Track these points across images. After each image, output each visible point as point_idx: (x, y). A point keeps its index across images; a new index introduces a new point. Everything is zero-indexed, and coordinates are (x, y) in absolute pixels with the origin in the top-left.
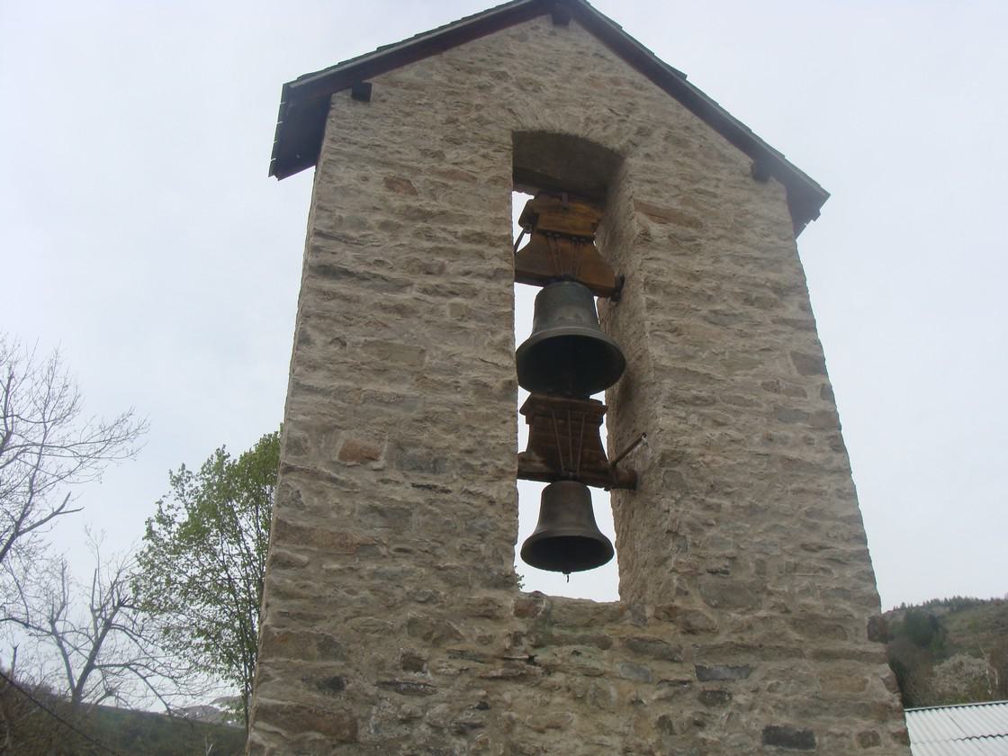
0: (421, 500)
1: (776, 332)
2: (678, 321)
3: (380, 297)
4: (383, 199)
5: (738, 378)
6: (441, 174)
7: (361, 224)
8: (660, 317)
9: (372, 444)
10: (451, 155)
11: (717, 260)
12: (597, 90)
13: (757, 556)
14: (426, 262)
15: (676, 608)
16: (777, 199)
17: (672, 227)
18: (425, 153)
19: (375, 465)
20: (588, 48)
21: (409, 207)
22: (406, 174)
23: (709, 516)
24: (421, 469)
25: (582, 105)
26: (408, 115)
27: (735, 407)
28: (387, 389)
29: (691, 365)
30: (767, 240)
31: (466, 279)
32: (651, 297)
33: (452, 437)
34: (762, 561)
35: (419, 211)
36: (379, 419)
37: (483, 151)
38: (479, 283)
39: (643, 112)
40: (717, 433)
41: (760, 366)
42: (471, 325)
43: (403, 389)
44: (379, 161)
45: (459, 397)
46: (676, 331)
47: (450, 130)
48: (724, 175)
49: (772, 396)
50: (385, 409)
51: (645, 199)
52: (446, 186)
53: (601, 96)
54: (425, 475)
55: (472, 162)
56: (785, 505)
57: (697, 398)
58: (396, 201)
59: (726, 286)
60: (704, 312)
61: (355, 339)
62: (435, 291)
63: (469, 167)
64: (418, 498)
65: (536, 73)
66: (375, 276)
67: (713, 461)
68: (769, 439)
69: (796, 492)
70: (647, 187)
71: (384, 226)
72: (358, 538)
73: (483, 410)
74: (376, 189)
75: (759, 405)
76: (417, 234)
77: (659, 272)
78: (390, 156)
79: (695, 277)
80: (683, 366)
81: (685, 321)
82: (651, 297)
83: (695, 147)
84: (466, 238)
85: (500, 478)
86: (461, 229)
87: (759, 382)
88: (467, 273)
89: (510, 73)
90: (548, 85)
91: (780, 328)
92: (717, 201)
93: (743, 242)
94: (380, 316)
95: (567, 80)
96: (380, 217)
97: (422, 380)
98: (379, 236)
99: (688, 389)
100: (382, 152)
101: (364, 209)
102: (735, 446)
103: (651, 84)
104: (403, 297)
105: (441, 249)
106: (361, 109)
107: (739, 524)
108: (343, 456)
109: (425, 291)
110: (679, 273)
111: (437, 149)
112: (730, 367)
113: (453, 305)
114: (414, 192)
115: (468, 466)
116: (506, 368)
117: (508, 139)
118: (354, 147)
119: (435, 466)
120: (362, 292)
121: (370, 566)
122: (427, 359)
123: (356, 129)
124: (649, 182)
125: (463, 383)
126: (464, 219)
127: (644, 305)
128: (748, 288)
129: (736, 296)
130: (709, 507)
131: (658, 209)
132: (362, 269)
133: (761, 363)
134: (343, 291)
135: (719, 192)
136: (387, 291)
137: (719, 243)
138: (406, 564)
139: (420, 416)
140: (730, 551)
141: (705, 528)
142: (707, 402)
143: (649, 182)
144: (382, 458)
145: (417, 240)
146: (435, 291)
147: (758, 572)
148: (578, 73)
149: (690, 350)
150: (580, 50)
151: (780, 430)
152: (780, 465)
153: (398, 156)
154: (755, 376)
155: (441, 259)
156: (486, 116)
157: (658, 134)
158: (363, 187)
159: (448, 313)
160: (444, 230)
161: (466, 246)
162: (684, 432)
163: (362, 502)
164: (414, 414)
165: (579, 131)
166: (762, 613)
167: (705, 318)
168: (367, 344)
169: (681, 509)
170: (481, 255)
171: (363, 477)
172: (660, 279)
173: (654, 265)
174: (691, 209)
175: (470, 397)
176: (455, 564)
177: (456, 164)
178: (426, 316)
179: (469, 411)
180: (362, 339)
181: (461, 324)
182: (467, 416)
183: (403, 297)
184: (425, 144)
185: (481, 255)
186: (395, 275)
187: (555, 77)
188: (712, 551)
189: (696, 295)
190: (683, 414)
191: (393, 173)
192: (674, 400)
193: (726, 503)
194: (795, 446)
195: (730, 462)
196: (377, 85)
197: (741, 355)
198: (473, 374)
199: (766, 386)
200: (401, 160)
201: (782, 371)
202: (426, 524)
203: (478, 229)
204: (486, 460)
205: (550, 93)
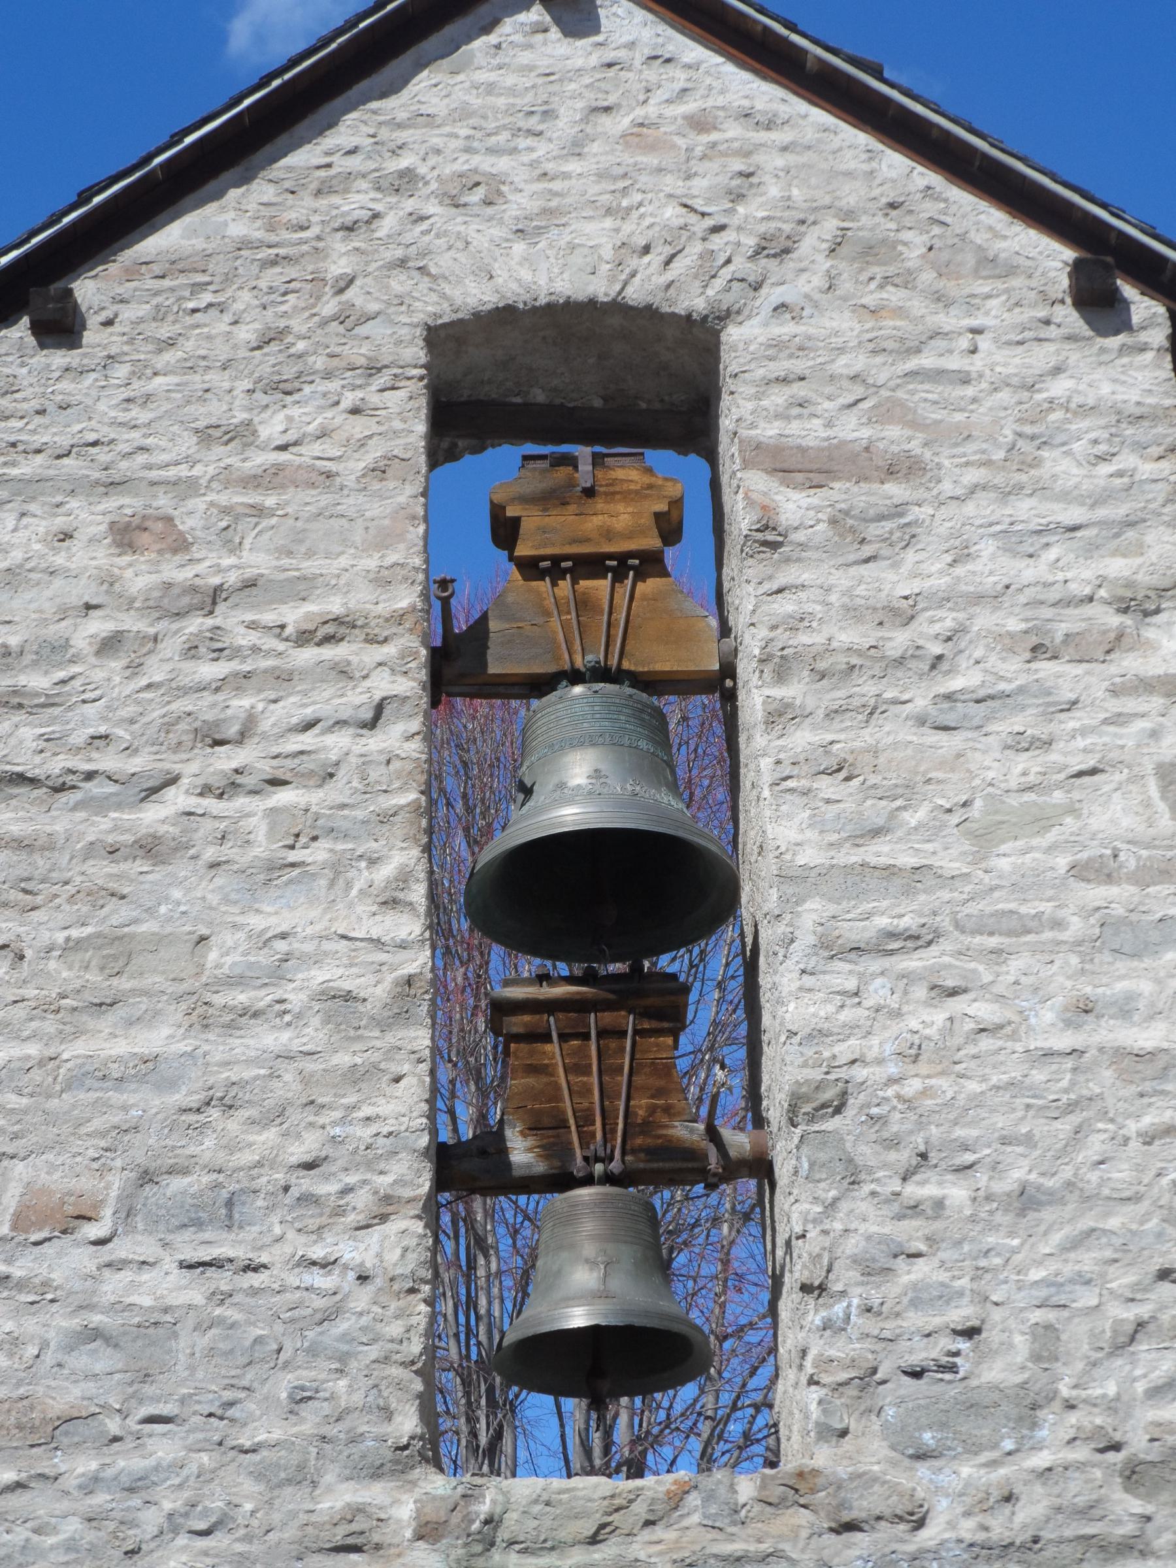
0: (196, 1297)
1: (1118, 720)
2: (849, 738)
3: (101, 827)
4: (109, 581)
5: (1004, 864)
6: (254, 481)
7: (55, 651)
8: (802, 738)
9: (86, 1183)
10: (272, 428)
11: (962, 555)
12: (652, 160)
13: (1037, 1316)
14: (209, 716)
15: (815, 1472)
16: (1143, 348)
17: (840, 492)
18: (206, 435)
19: (94, 1231)
20: (631, 45)
21: (168, 586)
22: (163, 502)
23: (911, 1233)
24: (198, 1224)
25: (609, 212)
26: (170, 343)
27: (993, 942)
28: (120, 1048)
29: (879, 852)
30: (1105, 469)
31: (307, 740)
32: (778, 692)
33: (271, 1135)
34: (1048, 1327)
35: (194, 590)
36: (97, 1124)
37: (350, 399)
38: (337, 743)
39: (774, 191)
40: (939, 1017)
41: (1068, 820)
42: (317, 854)
43: (156, 1039)
44: (97, 483)
45: (285, 1036)
46: (841, 769)
47: (267, 362)
48: (993, 315)
49: (1097, 894)
50: (115, 1097)
51: (768, 431)
52: (259, 511)
53: (660, 170)
54: (207, 1235)
55: (323, 434)
56: (1121, 1173)
57: (892, 935)
58: (141, 575)
59: (984, 620)
60: (921, 702)
61: (45, 937)
62: (229, 787)
63: (317, 448)
64: (192, 1293)
65: (491, 151)
66: (90, 776)
67: (925, 1092)
68: (1086, 1009)
69: (1148, 1139)
70: (778, 398)
71: (109, 645)
72: (58, 1405)
73: (343, 1059)
74: (90, 557)
75: (1058, 924)
76: (191, 651)
77: (799, 622)
78: (124, 464)
79: (903, 614)
80: (854, 857)
81: (868, 736)
82: (778, 692)
83: (913, 255)
84: (304, 638)
85: (383, 1218)
86: (293, 615)
87: (1062, 862)
88: (309, 726)
89: (422, 170)
90: (520, 176)
91: (1130, 705)
92: (970, 391)
93: (1040, 490)
94: (101, 871)
95: (576, 149)
96: (98, 626)
97: (203, 1019)
98: (98, 675)
99: (868, 916)
100: (102, 455)
101: (63, 613)
102: (986, 1043)
103: (798, 106)
104: (154, 816)
105: (247, 676)
106: (59, 358)
107: (991, 1240)
108: (19, 1222)
109: (206, 791)
110: (853, 613)
111: (241, 416)
112: (984, 839)
113: (273, 810)
114: (181, 545)
115: (308, 1199)
116: (403, 946)
117: (417, 353)
118: (39, 459)
119: (229, 1211)
120: (60, 820)
121: (86, 1464)
122: (213, 956)
123: (41, 412)
124: (784, 381)
125: (297, 999)
126: (301, 587)
127: (760, 715)
128: (1047, 612)
129: (1007, 643)
130: (915, 1209)
131: (803, 450)
132: (55, 765)
133: (1072, 810)
134: (15, 829)
135: (977, 364)
136: (119, 806)
137: (970, 508)
138: (164, 1447)
139: (194, 1100)
140: (961, 1314)
141: (901, 1263)
142: (915, 940)
143: (784, 381)
144: (107, 1212)
145: (188, 666)
146: (229, 787)
147: (1036, 1357)
148: (605, 121)
149: (875, 811)
150: (610, 55)
151: (1126, 980)
152: (1108, 1074)
153: (141, 459)
154: (1050, 849)
155: (246, 702)
156: (358, 302)
157: (812, 244)
158: (59, 560)
159: (261, 835)
160: (252, 626)
161: (308, 655)
162: (851, 1028)
163: (62, 1322)
164: (179, 1098)
165: (601, 288)
166: (1041, 1460)
167: (921, 721)
168: (72, 947)
169: (838, 1226)
170: (343, 672)
171: (66, 1263)
172: (804, 638)
173: (786, 606)
174: (894, 432)
175: (313, 1034)
176: (276, 1435)
177: (283, 448)
178: (211, 853)
179: (310, 1066)
180: (60, 937)
181: (293, 856)
182: (306, 1079)
183: (154, 816)
184: (212, 411)
185: (343, 672)
186: (136, 764)
187: (542, 149)
188: (915, 1320)
189: (900, 661)
190: (851, 984)
191: (127, 504)
192: (834, 949)
193: (957, 1193)
194: (1154, 1015)
195: (973, 1086)
196: (88, 290)
197: (1014, 801)
198: (319, 976)
199: (1079, 871)
200: (149, 467)
201: (1126, 822)
202: (211, 1353)
203: (335, 606)
204: (351, 1179)
205: (522, 202)
